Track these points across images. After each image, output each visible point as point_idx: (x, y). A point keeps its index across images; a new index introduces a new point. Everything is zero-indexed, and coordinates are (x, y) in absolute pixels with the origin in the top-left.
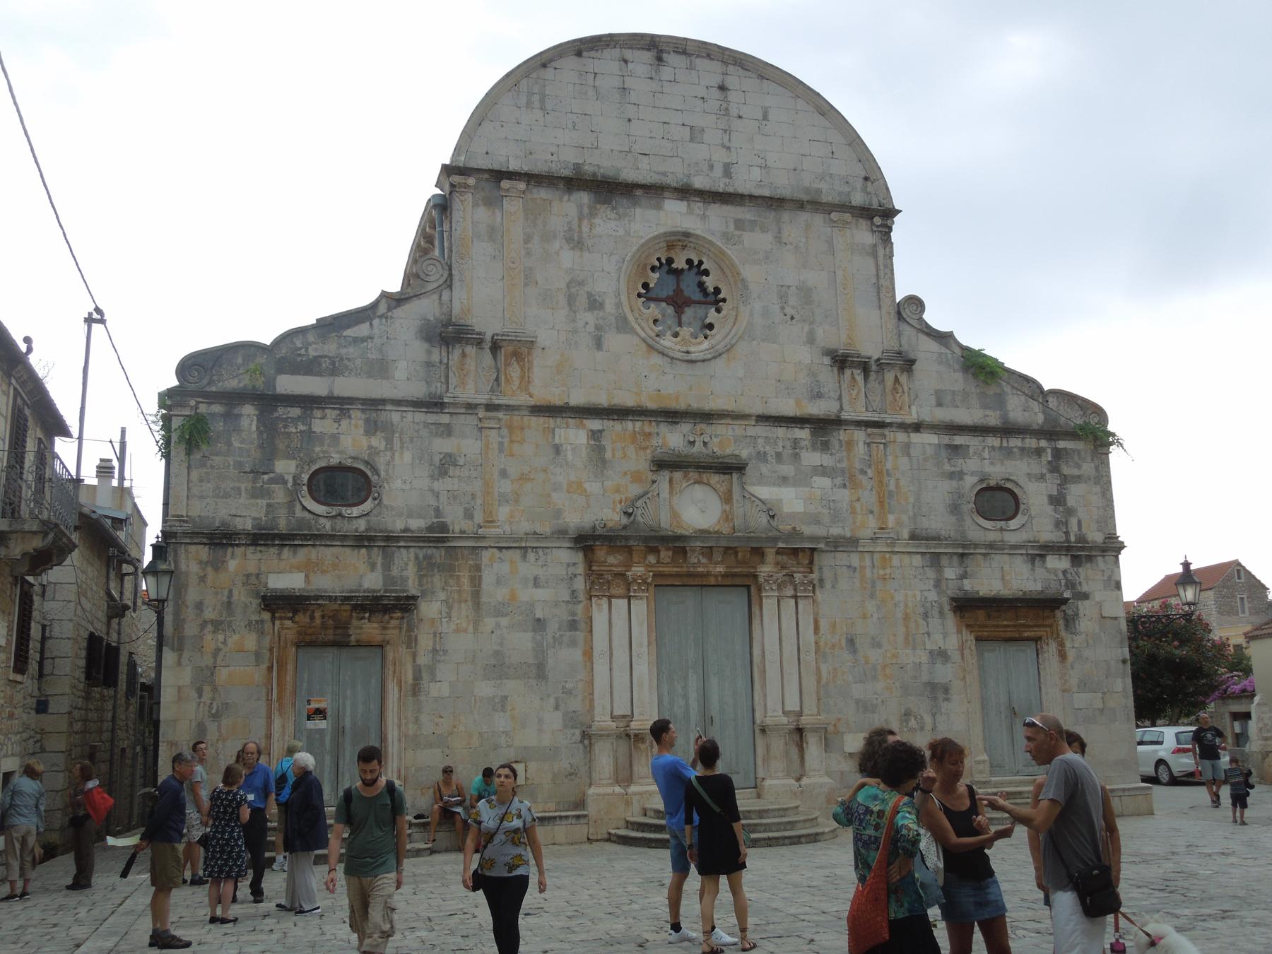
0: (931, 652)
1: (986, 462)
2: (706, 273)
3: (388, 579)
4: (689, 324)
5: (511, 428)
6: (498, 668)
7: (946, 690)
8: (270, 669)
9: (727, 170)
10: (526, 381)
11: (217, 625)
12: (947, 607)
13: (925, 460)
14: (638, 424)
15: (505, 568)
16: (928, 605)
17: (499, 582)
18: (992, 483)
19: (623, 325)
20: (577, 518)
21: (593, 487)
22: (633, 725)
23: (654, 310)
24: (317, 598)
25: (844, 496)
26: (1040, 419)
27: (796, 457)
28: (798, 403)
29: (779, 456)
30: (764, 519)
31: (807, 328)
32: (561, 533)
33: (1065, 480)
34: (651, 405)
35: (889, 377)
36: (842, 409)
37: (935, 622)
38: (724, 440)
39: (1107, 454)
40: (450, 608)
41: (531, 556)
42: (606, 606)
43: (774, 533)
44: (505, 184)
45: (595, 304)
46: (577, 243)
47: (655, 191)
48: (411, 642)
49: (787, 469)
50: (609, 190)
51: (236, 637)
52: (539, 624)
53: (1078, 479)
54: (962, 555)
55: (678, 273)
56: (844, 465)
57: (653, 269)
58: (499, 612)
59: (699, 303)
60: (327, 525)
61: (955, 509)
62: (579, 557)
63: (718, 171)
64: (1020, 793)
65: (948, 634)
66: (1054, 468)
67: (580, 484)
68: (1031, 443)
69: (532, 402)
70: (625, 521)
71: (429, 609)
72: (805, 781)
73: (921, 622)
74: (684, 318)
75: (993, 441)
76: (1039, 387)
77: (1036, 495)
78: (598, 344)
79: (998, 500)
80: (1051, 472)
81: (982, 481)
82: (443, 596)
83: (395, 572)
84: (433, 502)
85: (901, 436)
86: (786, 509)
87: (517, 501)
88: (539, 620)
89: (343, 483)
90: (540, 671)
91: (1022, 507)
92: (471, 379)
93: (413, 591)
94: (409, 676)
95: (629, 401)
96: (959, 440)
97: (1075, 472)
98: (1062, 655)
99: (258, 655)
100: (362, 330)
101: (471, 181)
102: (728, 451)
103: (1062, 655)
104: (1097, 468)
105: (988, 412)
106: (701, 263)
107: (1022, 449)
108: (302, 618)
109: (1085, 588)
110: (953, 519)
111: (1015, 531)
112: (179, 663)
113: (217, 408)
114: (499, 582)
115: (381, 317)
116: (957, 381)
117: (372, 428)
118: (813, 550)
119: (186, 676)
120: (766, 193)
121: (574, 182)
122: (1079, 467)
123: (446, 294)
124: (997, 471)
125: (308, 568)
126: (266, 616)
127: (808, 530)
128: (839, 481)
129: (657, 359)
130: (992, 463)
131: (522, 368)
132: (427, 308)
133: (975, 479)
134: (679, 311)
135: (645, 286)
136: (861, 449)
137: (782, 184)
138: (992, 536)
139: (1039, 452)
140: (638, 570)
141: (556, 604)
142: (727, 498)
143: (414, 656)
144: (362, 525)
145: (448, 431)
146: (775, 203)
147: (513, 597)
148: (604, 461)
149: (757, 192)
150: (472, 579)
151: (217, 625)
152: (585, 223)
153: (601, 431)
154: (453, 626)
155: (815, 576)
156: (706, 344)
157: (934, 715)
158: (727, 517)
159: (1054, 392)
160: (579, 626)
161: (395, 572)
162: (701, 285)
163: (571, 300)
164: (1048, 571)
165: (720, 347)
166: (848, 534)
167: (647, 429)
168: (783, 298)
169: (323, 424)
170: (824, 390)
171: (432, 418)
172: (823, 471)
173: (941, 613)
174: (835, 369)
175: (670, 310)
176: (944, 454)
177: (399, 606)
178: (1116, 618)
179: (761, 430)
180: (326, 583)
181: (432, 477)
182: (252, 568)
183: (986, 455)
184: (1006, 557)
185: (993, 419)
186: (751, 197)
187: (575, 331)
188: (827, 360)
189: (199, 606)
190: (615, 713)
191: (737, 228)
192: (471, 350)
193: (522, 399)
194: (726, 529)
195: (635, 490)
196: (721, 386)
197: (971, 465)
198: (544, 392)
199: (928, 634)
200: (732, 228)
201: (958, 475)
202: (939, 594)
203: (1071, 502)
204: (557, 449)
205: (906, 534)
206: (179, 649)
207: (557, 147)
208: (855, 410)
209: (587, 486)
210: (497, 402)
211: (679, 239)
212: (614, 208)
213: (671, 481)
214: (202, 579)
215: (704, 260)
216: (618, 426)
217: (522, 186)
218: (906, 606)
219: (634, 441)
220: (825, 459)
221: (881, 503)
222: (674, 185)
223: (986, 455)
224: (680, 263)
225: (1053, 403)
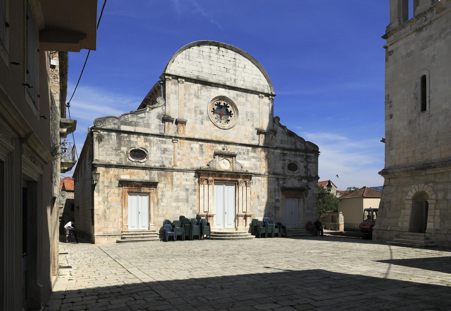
1: (290, 157)
2: (228, 107)
3: (150, 177)
4: (224, 120)
5: (180, 143)
8: (122, 198)
10: (184, 131)
11: (108, 187)
15: (179, 176)
17: (177, 179)
18: (292, 162)
19: (209, 118)
20: (197, 165)
21: (200, 158)
23: (215, 116)
24: (134, 181)
25: (258, 163)
27: (248, 154)
28: (249, 141)
29: (244, 153)
30: (240, 168)
31: (252, 123)
33: (308, 163)
34: (215, 139)
38: (231, 149)
40: (166, 185)
43: (242, 171)
45: (201, 113)
46: (197, 97)
47: (217, 85)
48: (157, 193)
49: (246, 157)
51: (113, 190)
55: (222, 106)
56: (259, 156)
57: (216, 105)
58: (177, 187)
60: (135, 164)
61: (283, 168)
63: (233, 81)
66: (306, 160)
67: (197, 157)
68: (301, 153)
75: (293, 153)
76: (304, 140)
77: (301, 166)
78: (202, 123)
79: (293, 167)
82: (164, 182)
83: (152, 176)
84: (161, 159)
85: (272, 150)
86: (245, 166)
87: (182, 160)
89: (139, 154)
92: (171, 129)
93: (157, 180)
94: (156, 201)
95: (209, 138)
96: (285, 152)
99: (118, 194)
107: (299, 155)
112: (99, 196)
114: (177, 179)
116: (286, 138)
119: (100, 199)
120: (244, 88)
123: (164, 107)
124: (293, 159)
125: (131, 174)
127: (250, 171)
128: (257, 160)
129: (216, 128)
131: (184, 128)
135: (213, 109)
137: (248, 86)
139: (303, 156)
141: (191, 185)
143: (157, 196)
147: (181, 183)
148: (203, 152)
149: (242, 87)
150: (171, 178)
151: (108, 187)
153: (202, 145)
154: (166, 189)
156: (228, 125)
159: (307, 142)
161: (152, 176)
162: (227, 110)
163: (195, 111)
165: (231, 126)
168: (247, 115)
170: (255, 138)
172: (254, 157)
175: (219, 116)
176: (282, 155)
177: (154, 185)
182: (116, 174)
185: (293, 147)
186: (241, 89)
187: (196, 120)
189: (103, 182)
191: (237, 96)
194: (231, 170)
195: (210, 159)
196: (230, 136)
197: (287, 158)
200: (235, 96)
201: (284, 160)
204: (192, 149)
206: (99, 192)
209: (199, 158)
212: (207, 88)
214: (104, 175)
216: (206, 144)
219: (210, 148)
220: (255, 155)
222: (222, 83)
225: (307, 144)
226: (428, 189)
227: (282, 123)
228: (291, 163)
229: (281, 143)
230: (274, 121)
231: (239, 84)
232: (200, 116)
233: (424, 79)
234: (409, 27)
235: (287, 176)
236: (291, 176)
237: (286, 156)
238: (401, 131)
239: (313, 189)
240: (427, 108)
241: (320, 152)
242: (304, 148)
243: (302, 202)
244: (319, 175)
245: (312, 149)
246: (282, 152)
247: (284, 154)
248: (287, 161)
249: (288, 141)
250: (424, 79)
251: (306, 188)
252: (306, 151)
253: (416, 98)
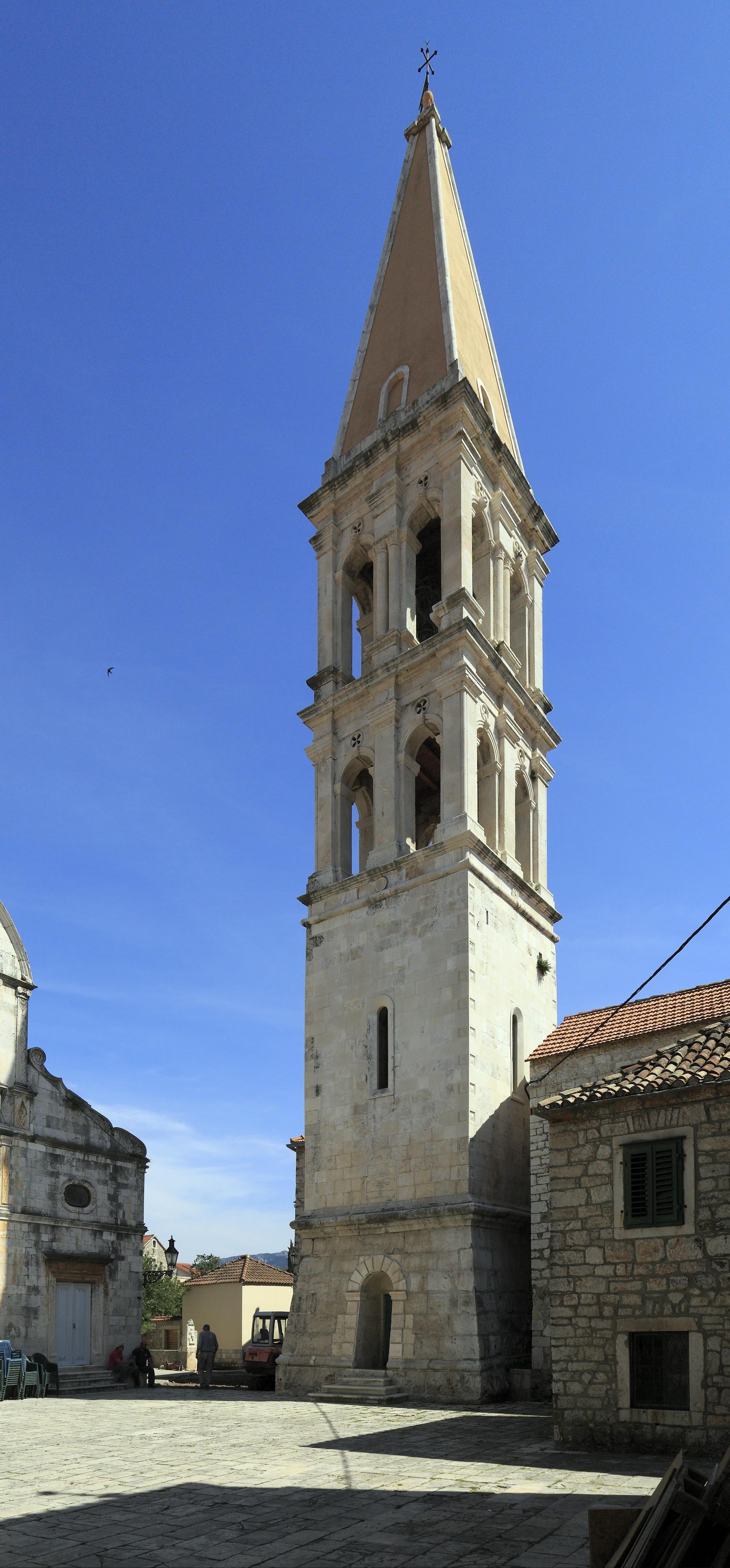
0: (29, 1287)
1: (72, 1168)
7: (36, 1311)
12: (41, 1259)
13: (36, 1161)
16: (29, 1257)
18: (76, 1182)
33: (119, 1186)
37: (33, 1268)
39: (144, 1173)
53: (125, 1186)
54: (53, 1227)
61: (52, 1196)
64: (76, 1375)
66: (113, 1178)
68: (102, 1160)
73: (24, 1268)
75: (79, 1155)
76: (110, 1124)
77: (101, 1193)
79: (78, 1195)
80: (111, 1180)
81: (70, 1180)
91: (92, 1200)
96: (58, 1152)
97: (125, 1182)
104: (137, 1180)
105: (78, 1136)
107: (96, 1163)
109: (123, 1253)
110: (50, 1203)
111: (86, 1214)
116: (61, 1112)
122: (127, 1179)
124: (80, 1174)
130: (77, 1170)
133: (66, 1178)
138: (73, 1216)
139: (106, 1166)
157: (27, 1327)
164: (104, 1241)
173: (37, 1263)
176: (48, 1159)
183: (74, 1164)
184: (80, 1231)
185: (81, 1140)
197: (64, 1168)
199: (28, 1276)
201: (55, 1175)
202: (37, 1250)
203: (121, 1200)
218: (15, 1257)
223: (74, 1164)
225: (117, 1136)
226: (391, 1268)
227: (53, 1067)
228: (74, 1185)
230: (28, 1061)
233: (383, 1015)
234: (355, 890)
235: (63, 1220)
236: (72, 1221)
237: (62, 1163)
238: (339, 1128)
239: (130, 1259)
240: (390, 1083)
241: (148, 1161)
242: (108, 1145)
243: (102, 1295)
244: (147, 1222)
245: (130, 1151)
246: (50, 1150)
247: (56, 1158)
248: (63, 1178)
249: (66, 1122)
250: (383, 1015)
251: (113, 1257)
252: (114, 1154)
253: (369, 1058)
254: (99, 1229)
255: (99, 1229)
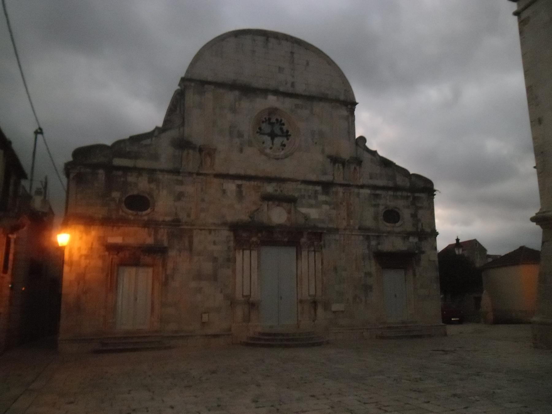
1: (388, 201)
6: (199, 276)
9: (293, 85)
14: (256, 183)
19: (250, 144)
22: (251, 299)
25: (334, 212)
26: (408, 185)
27: (316, 197)
29: (309, 196)
32: (225, 224)
35: (352, 167)
36: (334, 179)
38: (289, 189)
39: (433, 198)
41: (213, 232)
42: (241, 253)
44: (206, 86)
46: (233, 110)
47: (265, 92)
48: (164, 265)
49: (313, 202)
50: (247, 90)
52: (215, 259)
53: (421, 208)
57: (263, 122)
59: (280, 136)
61: (376, 218)
62: (232, 234)
63: (289, 85)
65: (372, 266)
68: (405, 194)
69: (215, 172)
70: (250, 220)
71: (172, 253)
72: (316, 322)
74: (274, 142)
75: (391, 193)
77: (406, 214)
78: (241, 151)
79: (392, 216)
81: (386, 208)
85: (356, 190)
86: (313, 217)
88: (215, 258)
90: (214, 277)
93: (166, 244)
96: (378, 192)
98: (414, 275)
100: (148, 141)
101: (193, 84)
102: (290, 194)
103: (414, 275)
106: (281, 121)
108: (121, 255)
109: (423, 250)
111: (398, 227)
113: (88, 170)
115: (156, 137)
117: (151, 181)
118: (321, 233)
120: (307, 94)
121: (233, 86)
124: (392, 204)
126: (107, 253)
127: (320, 225)
132: (173, 133)
133: (384, 207)
134: (273, 139)
135: (260, 129)
136: (341, 194)
138: (389, 229)
139: (408, 197)
140: (254, 239)
142: (289, 212)
144: (146, 218)
145: (181, 183)
146: (310, 98)
149: (303, 94)
152: (237, 103)
153: (241, 185)
155: (322, 243)
156: (282, 153)
158: (289, 219)
159: (414, 175)
160: (231, 260)
161: (159, 237)
162: (281, 129)
166: (335, 227)
167: (259, 185)
169: (131, 179)
171: (175, 177)
172: (326, 203)
174: (332, 164)
175: (269, 138)
178: (434, 261)
179: (302, 186)
180: (131, 241)
181: (175, 201)
185: (391, 184)
188: (329, 160)
190: (244, 294)
192: (191, 151)
193: (210, 172)
195: (254, 208)
196: (287, 168)
197: (382, 202)
198: (219, 168)
203: (419, 217)
204: (224, 192)
205: (357, 227)
207: (226, 71)
208: (339, 179)
210: (201, 172)
211: (273, 111)
213: (268, 205)
215: (283, 119)
217: (213, 87)
221: (348, 215)
224: (273, 120)
225: (413, 179)
229: (371, 178)
231: (300, 89)
232: (237, 140)
241: (435, 191)
242: (408, 185)
247: (377, 196)
252: (413, 189)
254: (406, 235)
255: (406, 235)
